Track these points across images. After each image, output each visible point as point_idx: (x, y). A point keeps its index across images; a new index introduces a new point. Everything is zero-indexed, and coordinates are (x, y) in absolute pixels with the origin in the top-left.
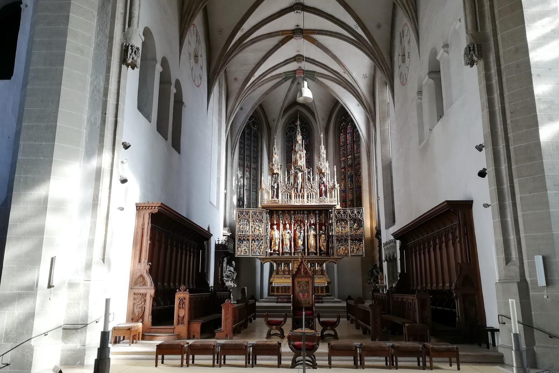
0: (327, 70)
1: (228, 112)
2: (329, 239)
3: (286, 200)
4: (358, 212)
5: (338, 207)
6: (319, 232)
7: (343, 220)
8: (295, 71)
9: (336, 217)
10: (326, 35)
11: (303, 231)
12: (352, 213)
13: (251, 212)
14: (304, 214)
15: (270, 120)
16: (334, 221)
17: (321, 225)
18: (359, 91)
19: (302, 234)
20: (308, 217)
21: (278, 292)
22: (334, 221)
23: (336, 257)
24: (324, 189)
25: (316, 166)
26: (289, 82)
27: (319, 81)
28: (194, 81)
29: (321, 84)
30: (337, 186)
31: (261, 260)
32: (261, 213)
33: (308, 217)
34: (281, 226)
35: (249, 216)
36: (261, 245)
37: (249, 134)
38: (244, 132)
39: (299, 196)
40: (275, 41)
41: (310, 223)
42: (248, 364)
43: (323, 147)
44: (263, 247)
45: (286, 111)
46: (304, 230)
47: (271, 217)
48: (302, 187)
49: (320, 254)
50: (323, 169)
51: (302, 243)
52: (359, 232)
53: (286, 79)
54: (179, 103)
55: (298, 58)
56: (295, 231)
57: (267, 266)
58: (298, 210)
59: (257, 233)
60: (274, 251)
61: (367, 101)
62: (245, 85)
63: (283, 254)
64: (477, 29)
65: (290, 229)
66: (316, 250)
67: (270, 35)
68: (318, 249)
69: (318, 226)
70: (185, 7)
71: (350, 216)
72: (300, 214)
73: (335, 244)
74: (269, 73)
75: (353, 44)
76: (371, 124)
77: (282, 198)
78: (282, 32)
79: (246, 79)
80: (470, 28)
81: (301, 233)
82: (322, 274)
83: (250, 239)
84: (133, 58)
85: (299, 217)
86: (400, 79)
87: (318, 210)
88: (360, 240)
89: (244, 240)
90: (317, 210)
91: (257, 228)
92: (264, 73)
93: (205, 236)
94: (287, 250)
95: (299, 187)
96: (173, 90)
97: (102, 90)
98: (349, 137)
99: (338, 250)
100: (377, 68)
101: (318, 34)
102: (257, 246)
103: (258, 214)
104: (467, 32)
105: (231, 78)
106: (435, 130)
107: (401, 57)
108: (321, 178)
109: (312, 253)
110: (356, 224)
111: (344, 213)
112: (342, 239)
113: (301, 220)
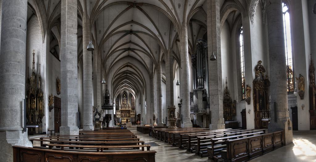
2: (130, 115)
57: (121, 119)
85: (125, 111)
112: (132, 115)
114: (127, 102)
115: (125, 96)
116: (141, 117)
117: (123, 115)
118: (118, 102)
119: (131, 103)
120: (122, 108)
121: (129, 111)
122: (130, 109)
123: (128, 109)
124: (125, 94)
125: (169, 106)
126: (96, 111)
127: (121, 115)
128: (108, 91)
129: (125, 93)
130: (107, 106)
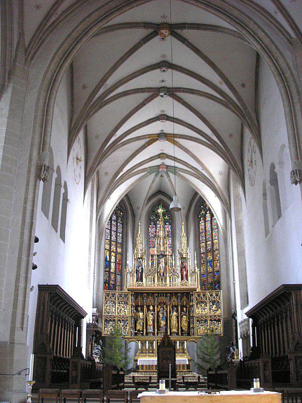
0: (187, 166)
1: (99, 203)
3: (150, 283)
4: (217, 295)
5: (198, 290)
6: (181, 313)
7: (202, 302)
8: (159, 166)
9: (197, 300)
10: (186, 139)
11: (165, 313)
12: (211, 295)
13: (117, 294)
14: (166, 296)
15: (135, 208)
17: (182, 307)
18: (216, 186)
19: (165, 315)
20: (170, 299)
21: (142, 369)
23: (197, 337)
24: (185, 273)
25: (177, 251)
26: (153, 175)
27: (180, 175)
28: (75, 180)
29: (182, 177)
30: (197, 270)
31: (126, 339)
32: (126, 296)
33: (170, 299)
34: (145, 309)
35: (115, 298)
36: (126, 326)
37: (116, 221)
38: (111, 219)
39: (162, 279)
40: (142, 142)
41: (172, 305)
43: (184, 233)
44: (128, 327)
45: (149, 199)
46: (167, 312)
47: (136, 299)
48: (165, 270)
49: (182, 334)
50: (184, 255)
51: (165, 323)
52: (218, 313)
53: (150, 173)
54: (66, 200)
55: (161, 156)
56: (158, 312)
58: (161, 293)
59: (122, 314)
60: (139, 331)
61: (222, 195)
62: (115, 179)
63: (147, 334)
64: (298, 159)
65: (154, 310)
66: (178, 330)
67: (138, 138)
68: (180, 330)
69: (179, 308)
70: (74, 122)
71: (209, 298)
72: (163, 296)
73: (196, 324)
74: (136, 168)
75: (209, 147)
76: (227, 215)
77: (146, 281)
78: (149, 136)
79: (115, 174)
80: (293, 157)
81: (163, 314)
82: (184, 352)
84: (45, 175)
85: (163, 299)
86: (250, 179)
87: (180, 293)
88: (219, 320)
89: (110, 320)
90: (179, 293)
91: (123, 309)
92: (131, 168)
93: (79, 315)
94: (151, 330)
95: (162, 271)
96: (63, 191)
97: (23, 199)
98: (208, 224)
99: (199, 330)
100: (231, 170)
101: (179, 138)
102: (123, 326)
103: (123, 296)
104: (291, 160)
105: (102, 173)
106: (276, 226)
107: (249, 163)
108: (182, 263)
109: (174, 333)
110: (214, 306)
111: (204, 296)
112: (202, 320)
113: (163, 302)
115: (164, 214)
118: (124, 245)
119: (197, 248)
121: (187, 294)
122: (193, 283)
123: (177, 284)
124: (159, 203)
129: (161, 196)
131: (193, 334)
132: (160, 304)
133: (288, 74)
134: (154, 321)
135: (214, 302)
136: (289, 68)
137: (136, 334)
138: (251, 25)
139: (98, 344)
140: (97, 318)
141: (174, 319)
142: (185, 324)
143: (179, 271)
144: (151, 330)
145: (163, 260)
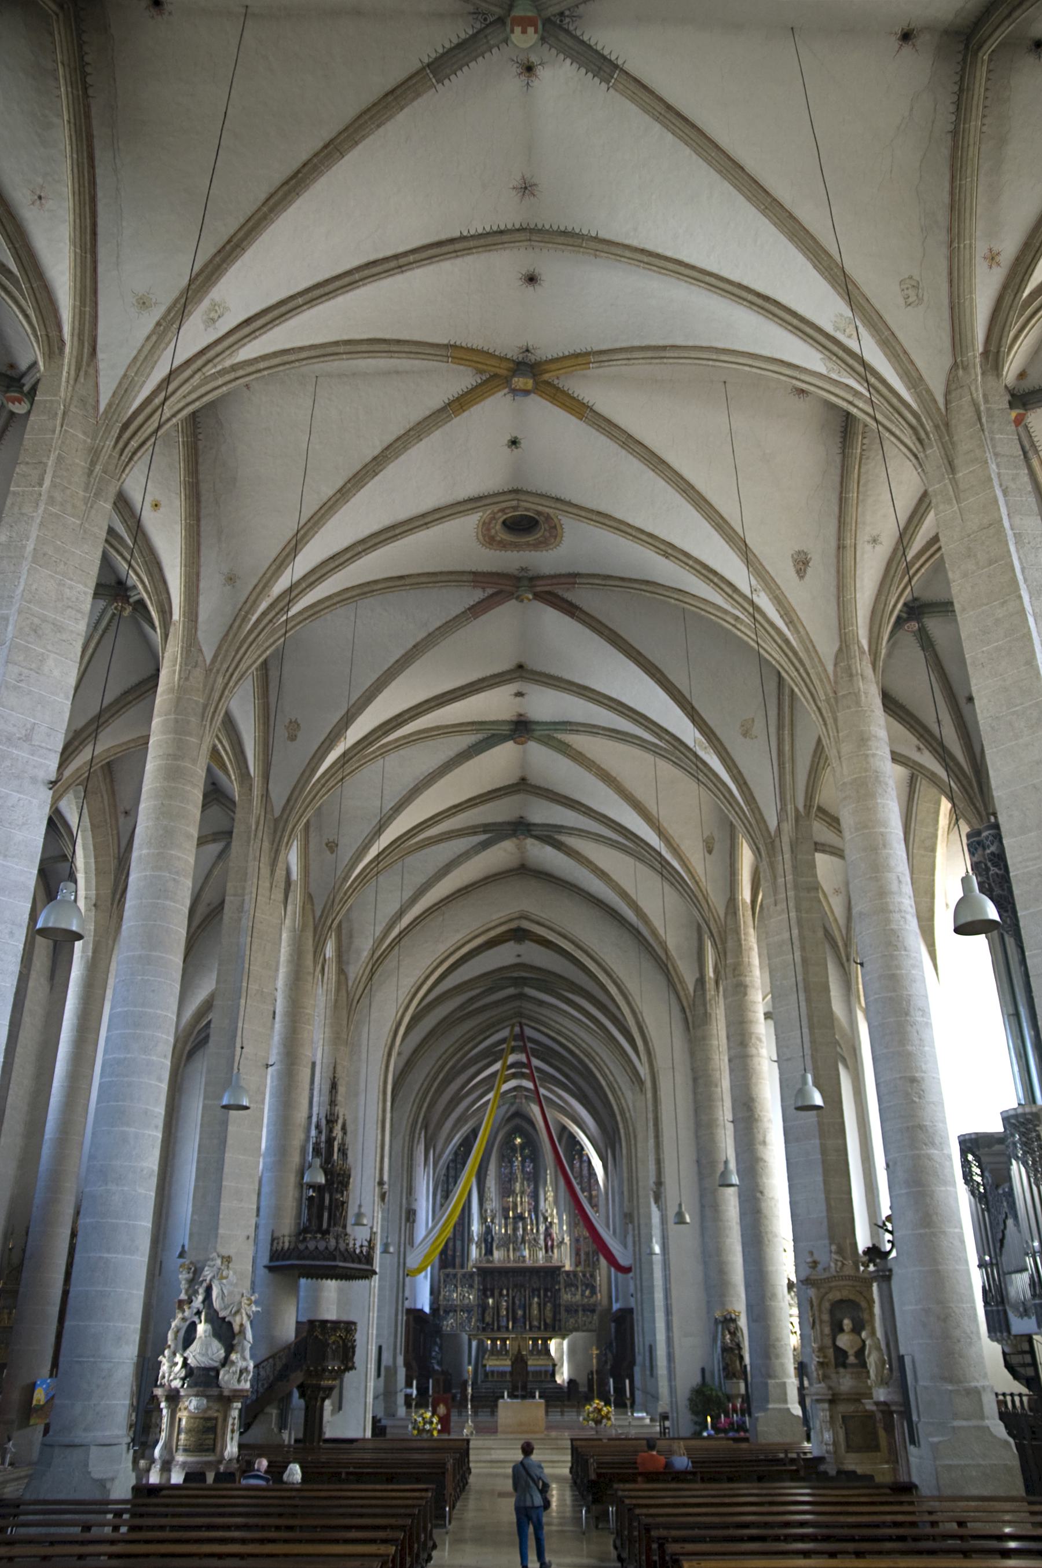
2: (556, 1308)
7: (572, 1285)
12: (584, 1276)
13: (459, 1275)
16: (562, 1286)
17: (546, 1290)
22: (562, 1286)
24: (550, 1243)
30: (567, 1239)
42: (449, 1466)
49: (546, 1329)
56: (513, 1298)
59: (466, 1301)
60: (488, 1324)
63: (499, 1329)
65: (508, 1295)
69: (542, 1292)
73: (564, 1315)
83: (458, 1309)
88: (593, 1311)
95: (520, 1240)
98: (585, 1165)
108: (547, 1229)
114: (535, 1196)
115: (523, 1146)
116: (638, 1339)
117: (497, 1307)
120: (489, 1252)
121: (552, 1273)
124: (518, 1131)
125: (815, 1264)
126: (198, 1301)
127: (484, 1307)
128: (337, 1131)
130: (316, 1254)
131: (560, 1329)
132: (515, 1286)
133: (628, 1115)
134: (507, 1309)
135: (587, 1286)
136: (629, 1111)
137: (484, 1329)
138: (598, 1059)
139: (435, 1343)
140: (435, 1309)
141: (535, 1306)
142: (549, 1314)
143: (542, 1242)
144: (503, 1323)
145: (520, 1224)
